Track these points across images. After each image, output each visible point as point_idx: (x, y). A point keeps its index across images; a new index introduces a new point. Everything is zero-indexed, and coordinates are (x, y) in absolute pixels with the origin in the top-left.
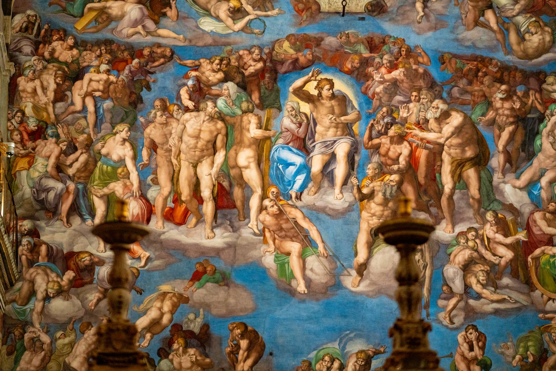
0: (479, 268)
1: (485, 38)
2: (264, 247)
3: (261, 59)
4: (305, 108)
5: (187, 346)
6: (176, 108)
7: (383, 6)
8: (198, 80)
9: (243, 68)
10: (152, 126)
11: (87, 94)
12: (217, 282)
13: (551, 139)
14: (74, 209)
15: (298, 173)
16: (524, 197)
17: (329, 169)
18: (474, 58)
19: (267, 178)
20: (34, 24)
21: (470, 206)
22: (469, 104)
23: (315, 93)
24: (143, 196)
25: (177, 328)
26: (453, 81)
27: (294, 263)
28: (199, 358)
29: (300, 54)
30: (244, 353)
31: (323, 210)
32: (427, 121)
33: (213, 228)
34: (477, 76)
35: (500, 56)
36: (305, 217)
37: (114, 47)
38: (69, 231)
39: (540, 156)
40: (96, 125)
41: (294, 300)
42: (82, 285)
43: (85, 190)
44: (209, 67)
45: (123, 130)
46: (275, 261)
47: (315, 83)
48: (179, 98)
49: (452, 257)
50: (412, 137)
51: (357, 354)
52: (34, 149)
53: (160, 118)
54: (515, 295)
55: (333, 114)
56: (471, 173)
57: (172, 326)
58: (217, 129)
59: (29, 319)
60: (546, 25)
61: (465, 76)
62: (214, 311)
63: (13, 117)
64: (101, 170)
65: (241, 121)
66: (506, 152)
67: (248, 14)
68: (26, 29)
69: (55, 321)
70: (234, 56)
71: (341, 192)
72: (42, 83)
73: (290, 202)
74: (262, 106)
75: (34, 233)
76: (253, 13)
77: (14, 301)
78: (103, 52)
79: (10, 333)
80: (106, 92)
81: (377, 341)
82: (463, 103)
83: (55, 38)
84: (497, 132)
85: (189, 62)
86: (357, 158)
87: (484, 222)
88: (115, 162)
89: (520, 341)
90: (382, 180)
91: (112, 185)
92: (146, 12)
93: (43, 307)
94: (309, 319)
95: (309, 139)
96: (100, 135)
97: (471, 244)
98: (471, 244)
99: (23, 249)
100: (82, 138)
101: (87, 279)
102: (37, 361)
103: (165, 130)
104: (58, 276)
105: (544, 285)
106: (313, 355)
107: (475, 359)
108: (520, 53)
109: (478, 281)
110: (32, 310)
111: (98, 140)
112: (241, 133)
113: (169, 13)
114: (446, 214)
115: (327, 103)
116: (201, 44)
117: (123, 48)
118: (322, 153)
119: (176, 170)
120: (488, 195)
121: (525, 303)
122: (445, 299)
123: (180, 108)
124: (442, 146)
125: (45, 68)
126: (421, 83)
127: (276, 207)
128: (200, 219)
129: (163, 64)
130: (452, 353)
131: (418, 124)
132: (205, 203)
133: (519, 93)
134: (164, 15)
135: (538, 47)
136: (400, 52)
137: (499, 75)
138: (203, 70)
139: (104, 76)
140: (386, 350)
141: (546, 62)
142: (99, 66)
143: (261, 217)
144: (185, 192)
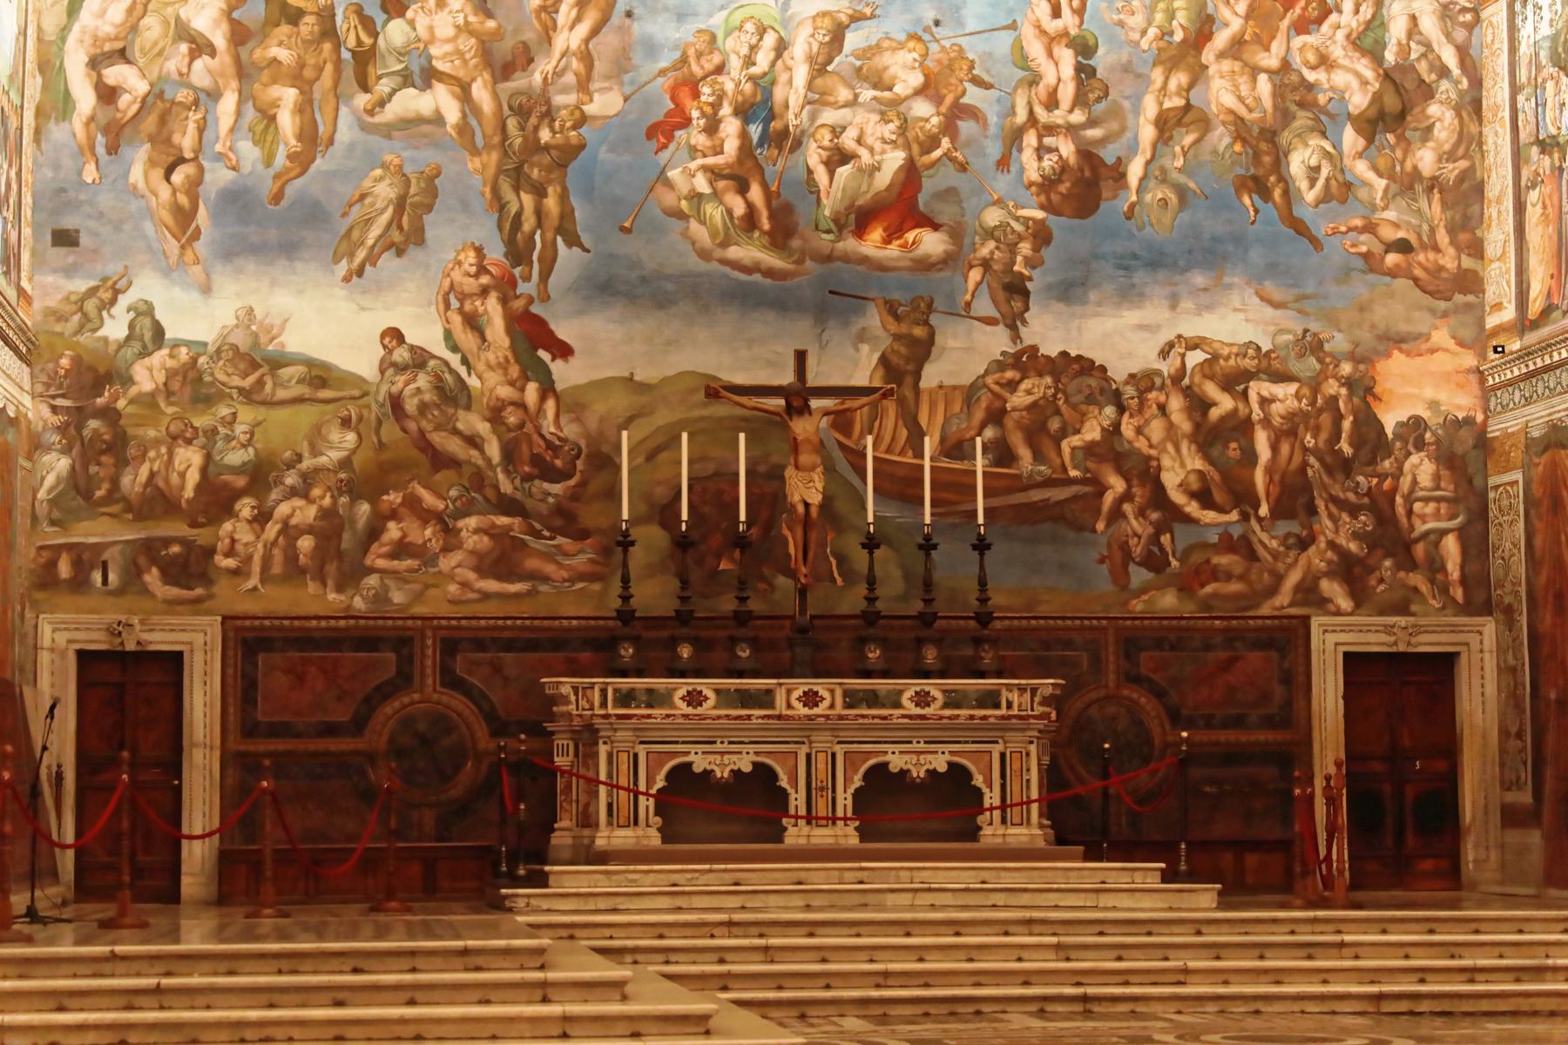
28: (472, 19)
30: (570, 11)
51: (814, 18)
107: (1065, 34)
130: (1015, 21)
140: (878, 12)
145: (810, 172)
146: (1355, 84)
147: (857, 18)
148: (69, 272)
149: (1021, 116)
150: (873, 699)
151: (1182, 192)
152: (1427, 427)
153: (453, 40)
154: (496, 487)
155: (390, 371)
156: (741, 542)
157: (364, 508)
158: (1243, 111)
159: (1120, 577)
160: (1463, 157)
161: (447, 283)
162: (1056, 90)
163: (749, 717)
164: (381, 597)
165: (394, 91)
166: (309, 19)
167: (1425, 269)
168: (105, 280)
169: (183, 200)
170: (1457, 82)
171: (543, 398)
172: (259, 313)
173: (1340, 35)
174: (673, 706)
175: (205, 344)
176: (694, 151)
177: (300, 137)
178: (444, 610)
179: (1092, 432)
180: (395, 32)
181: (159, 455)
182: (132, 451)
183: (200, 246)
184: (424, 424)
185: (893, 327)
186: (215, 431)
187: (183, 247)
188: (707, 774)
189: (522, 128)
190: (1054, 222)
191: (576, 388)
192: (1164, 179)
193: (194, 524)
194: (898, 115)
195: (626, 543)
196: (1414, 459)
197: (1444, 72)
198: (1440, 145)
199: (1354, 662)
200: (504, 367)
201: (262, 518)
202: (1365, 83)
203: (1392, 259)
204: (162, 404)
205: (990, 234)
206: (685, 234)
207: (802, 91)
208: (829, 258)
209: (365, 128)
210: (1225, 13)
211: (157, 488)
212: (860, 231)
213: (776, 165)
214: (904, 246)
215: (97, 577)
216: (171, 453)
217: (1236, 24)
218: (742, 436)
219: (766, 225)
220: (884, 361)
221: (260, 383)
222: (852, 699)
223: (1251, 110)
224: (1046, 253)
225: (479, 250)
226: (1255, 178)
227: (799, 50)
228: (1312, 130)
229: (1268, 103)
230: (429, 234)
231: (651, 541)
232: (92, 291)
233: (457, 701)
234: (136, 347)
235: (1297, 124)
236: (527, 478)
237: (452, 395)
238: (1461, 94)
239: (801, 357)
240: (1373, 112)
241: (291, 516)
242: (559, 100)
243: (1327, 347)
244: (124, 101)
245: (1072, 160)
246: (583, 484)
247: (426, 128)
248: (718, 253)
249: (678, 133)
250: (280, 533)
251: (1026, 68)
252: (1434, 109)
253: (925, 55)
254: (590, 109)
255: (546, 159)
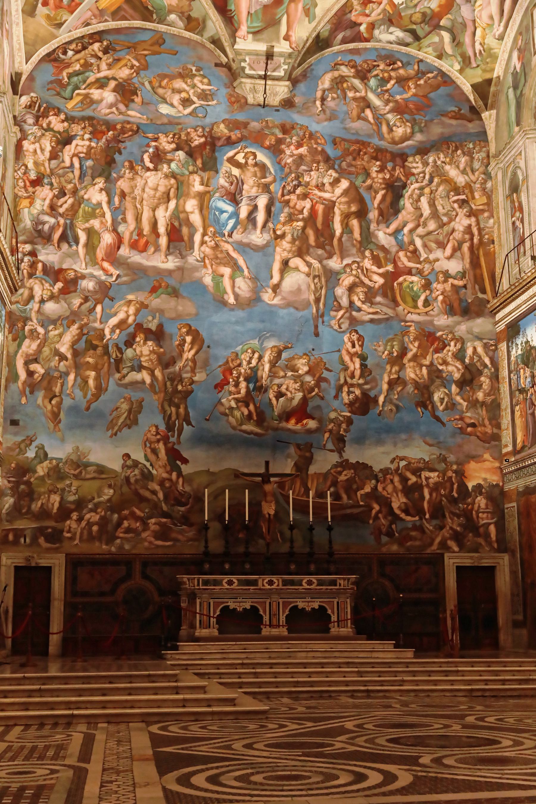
0: (359, 290)
1: (364, 128)
2: (204, 271)
3: (203, 136)
4: (236, 172)
5: (146, 340)
6: (140, 167)
7: (292, 102)
8: (157, 148)
9: (190, 141)
10: (122, 180)
11: (74, 155)
12: (169, 294)
13: (411, 201)
14: (64, 238)
15: (230, 218)
16: (392, 240)
17: (253, 216)
18: (357, 142)
19: (207, 221)
20: (36, 103)
21: (354, 245)
22: (353, 174)
23: (243, 161)
24: (115, 230)
25: (139, 327)
26: (342, 157)
27: (227, 283)
28: (155, 348)
29: (232, 133)
31: (248, 245)
32: (323, 185)
33: (166, 256)
34: (359, 154)
35: (375, 141)
36: (234, 250)
37: (95, 122)
38: (59, 253)
39: (403, 212)
40: (80, 178)
41: (226, 309)
42: (69, 293)
43: (72, 224)
44: (165, 139)
45: (100, 182)
46: (212, 281)
47: (243, 154)
48: (142, 160)
49: (341, 281)
50: (313, 195)
51: (271, 348)
52: (34, 193)
53: (128, 174)
54: (385, 309)
55: (256, 176)
56: (355, 223)
57: (136, 325)
58: (171, 184)
59: (29, 316)
60: (407, 121)
61: (351, 154)
62: (167, 315)
63: (19, 170)
64: (84, 210)
65: (189, 179)
66: (379, 208)
67: (194, 103)
68: (30, 107)
69: (48, 318)
70: (184, 133)
71: (261, 233)
72: (40, 145)
73: (224, 239)
74: (204, 169)
75: (33, 254)
76: (198, 103)
77: (17, 302)
78: (87, 125)
79: (15, 325)
80: (88, 155)
81: (286, 340)
82: (350, 173)
83: (51, 113)
84: (374, 194)
85: (150, 135)
86: (273, 209)
87: (364, 257)
88: (94, 205)
89: (388, 341)
90: (291, 225)
91: (92, 222)
92: (119, 98)
93: (40, 307)
94: (237, 323)
95: (238, 194)
96: (83, 185)
97: (354, 272)
98: (354, 272)
99: (24, 266)
100: (70, 186)
101: (72, 289)
102: (34, 346)
103: (132, 183)
104: (51, 285)
105: (405, 302)
106: (239, 348)
107: (356, 353)
108: (390, 140)
109: (359, 299)
110: (31, 310)
111: (82, 189)
112: (188, 188)
113: (136, 100)
114: (337, 251)
115: (252, 169)
116: (159, 122)
117: (101, 123)
118: (248, 205)
119: (140, 212)
120: (367, 239)
121: (392, 315)
122: (336, 311)
123: (143, 168)
124: (334, 203)
125: (43, 135)
126: (320, 157)
127: (213, 242)
128: (157, 249)
129: (131, 136)
131: (317, 187)
132: (161, 237)
133: (389, 168)
134: (133, 101)
135: (402, 136)
136: (304, 135)
137: (374, 154)
138: (160, 141)
139: (87, 143)
141: (407, 147)
142: (83, 135)
143: (203, 249)
144: (146, 228)
145: (270, 400)
146: (455, 370)
147: (286, 348)
148: (16, 434)
149: (342, 381)
150: (292, 583)
151: (397, 407)
152: (483, 487)
153: (149, 355)
154: (162, 508)
155: (126, 468)
156: (246, 528)
157: (116, 516)
158: (417, 379)
159: (378, 539)
160: (493, 395)
161: (145, 439)
162: (354, 372)
163: (249, 589)
164: (121, 547)
165: (128, 373)
166: (100, 348)
167: (481, 433)
168: (28, 437)
169: (55, 409)
170: (490, 369)
171: (178, 478)
172: (80, 448)
173: (450, 354)
174: (223, 586)
175: (62, 459)
176: (230, 393)
177: (96, 388)
178: (143, 552)
179: (368, 489)
180: (129, 353)
181: (45, 497)
182: (35, 496)
183: (60, 425)
184: (138, 487)
185: (299, 452)
186: (64, 489)
187: (55, 426)
188: (235, 609)
189: (172, 385)
190: (354, 417)
191: (190, 474)
192: (391, 402)
193: (57, 522)
194: (300, 380)
195: (206, 528)
196: (479, 498)
197: (486, 366)
198: (485, 390)
199: (460, 569)
200: (165, 467)
201: (80, 519)
202: (459, 370)
203: (469, 429)
204: (47, 480)
205: (332, 421)
206: (228, 421)
207: (267, 373)
208: (276, 429)
209: (119, 385)
210: (411, 346)
211: (45, 510)
212: (287, 420)
213: (259, 398)
214: (302, 425)
215: (22, 540)
216: (49, 497)
217: (415, 350)
218: (247, 491)
219: (255, 418)
220: (296, 464)
221: (81, 472)
222: (285, 583)
223: (420, 379)
224: (352, 427)
225: (157, 427)
226: (422, 402)
227: (266, 358)
228: (441, 385)
229: (426, 376)
230: (140, 421)
231: (215, 527)
232: (23, 441)
233: (147, 584)
234: (38, 460)
235: (436, 384)
236: (173, 505)
237: (147, 476)
238: (491, 373)
239: (267, 463)
240: (461, 380)
241: (90, 519)
242: (185, 375)
243: (448, 459)
244: (36, 375)
245: (360, 396)
246: (192, 507)
247: (139, 385)
248: (239, 428)
249: (225, 387)
250: (86, 525)
251: (344, 365)
252: (482, 379)
253: (309, 361)
254: (195, 379)
255: (180, 396)
